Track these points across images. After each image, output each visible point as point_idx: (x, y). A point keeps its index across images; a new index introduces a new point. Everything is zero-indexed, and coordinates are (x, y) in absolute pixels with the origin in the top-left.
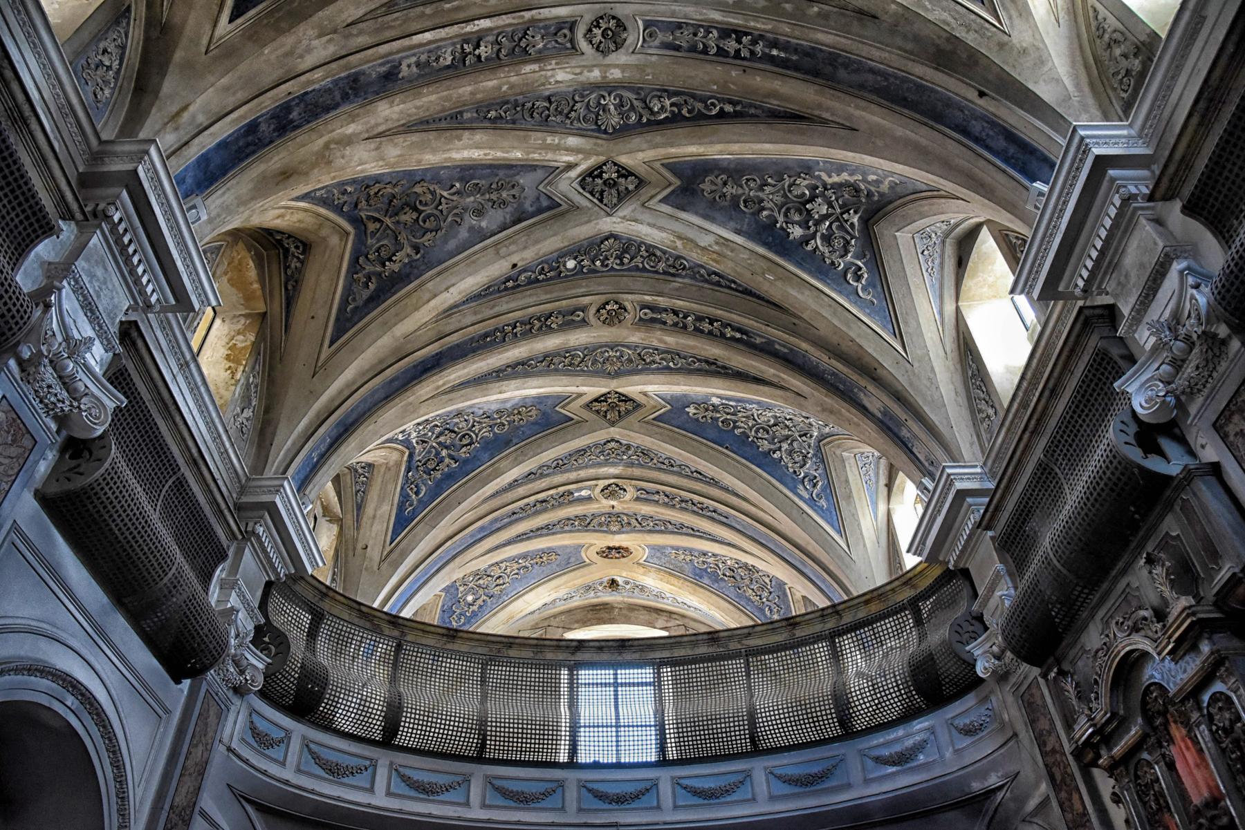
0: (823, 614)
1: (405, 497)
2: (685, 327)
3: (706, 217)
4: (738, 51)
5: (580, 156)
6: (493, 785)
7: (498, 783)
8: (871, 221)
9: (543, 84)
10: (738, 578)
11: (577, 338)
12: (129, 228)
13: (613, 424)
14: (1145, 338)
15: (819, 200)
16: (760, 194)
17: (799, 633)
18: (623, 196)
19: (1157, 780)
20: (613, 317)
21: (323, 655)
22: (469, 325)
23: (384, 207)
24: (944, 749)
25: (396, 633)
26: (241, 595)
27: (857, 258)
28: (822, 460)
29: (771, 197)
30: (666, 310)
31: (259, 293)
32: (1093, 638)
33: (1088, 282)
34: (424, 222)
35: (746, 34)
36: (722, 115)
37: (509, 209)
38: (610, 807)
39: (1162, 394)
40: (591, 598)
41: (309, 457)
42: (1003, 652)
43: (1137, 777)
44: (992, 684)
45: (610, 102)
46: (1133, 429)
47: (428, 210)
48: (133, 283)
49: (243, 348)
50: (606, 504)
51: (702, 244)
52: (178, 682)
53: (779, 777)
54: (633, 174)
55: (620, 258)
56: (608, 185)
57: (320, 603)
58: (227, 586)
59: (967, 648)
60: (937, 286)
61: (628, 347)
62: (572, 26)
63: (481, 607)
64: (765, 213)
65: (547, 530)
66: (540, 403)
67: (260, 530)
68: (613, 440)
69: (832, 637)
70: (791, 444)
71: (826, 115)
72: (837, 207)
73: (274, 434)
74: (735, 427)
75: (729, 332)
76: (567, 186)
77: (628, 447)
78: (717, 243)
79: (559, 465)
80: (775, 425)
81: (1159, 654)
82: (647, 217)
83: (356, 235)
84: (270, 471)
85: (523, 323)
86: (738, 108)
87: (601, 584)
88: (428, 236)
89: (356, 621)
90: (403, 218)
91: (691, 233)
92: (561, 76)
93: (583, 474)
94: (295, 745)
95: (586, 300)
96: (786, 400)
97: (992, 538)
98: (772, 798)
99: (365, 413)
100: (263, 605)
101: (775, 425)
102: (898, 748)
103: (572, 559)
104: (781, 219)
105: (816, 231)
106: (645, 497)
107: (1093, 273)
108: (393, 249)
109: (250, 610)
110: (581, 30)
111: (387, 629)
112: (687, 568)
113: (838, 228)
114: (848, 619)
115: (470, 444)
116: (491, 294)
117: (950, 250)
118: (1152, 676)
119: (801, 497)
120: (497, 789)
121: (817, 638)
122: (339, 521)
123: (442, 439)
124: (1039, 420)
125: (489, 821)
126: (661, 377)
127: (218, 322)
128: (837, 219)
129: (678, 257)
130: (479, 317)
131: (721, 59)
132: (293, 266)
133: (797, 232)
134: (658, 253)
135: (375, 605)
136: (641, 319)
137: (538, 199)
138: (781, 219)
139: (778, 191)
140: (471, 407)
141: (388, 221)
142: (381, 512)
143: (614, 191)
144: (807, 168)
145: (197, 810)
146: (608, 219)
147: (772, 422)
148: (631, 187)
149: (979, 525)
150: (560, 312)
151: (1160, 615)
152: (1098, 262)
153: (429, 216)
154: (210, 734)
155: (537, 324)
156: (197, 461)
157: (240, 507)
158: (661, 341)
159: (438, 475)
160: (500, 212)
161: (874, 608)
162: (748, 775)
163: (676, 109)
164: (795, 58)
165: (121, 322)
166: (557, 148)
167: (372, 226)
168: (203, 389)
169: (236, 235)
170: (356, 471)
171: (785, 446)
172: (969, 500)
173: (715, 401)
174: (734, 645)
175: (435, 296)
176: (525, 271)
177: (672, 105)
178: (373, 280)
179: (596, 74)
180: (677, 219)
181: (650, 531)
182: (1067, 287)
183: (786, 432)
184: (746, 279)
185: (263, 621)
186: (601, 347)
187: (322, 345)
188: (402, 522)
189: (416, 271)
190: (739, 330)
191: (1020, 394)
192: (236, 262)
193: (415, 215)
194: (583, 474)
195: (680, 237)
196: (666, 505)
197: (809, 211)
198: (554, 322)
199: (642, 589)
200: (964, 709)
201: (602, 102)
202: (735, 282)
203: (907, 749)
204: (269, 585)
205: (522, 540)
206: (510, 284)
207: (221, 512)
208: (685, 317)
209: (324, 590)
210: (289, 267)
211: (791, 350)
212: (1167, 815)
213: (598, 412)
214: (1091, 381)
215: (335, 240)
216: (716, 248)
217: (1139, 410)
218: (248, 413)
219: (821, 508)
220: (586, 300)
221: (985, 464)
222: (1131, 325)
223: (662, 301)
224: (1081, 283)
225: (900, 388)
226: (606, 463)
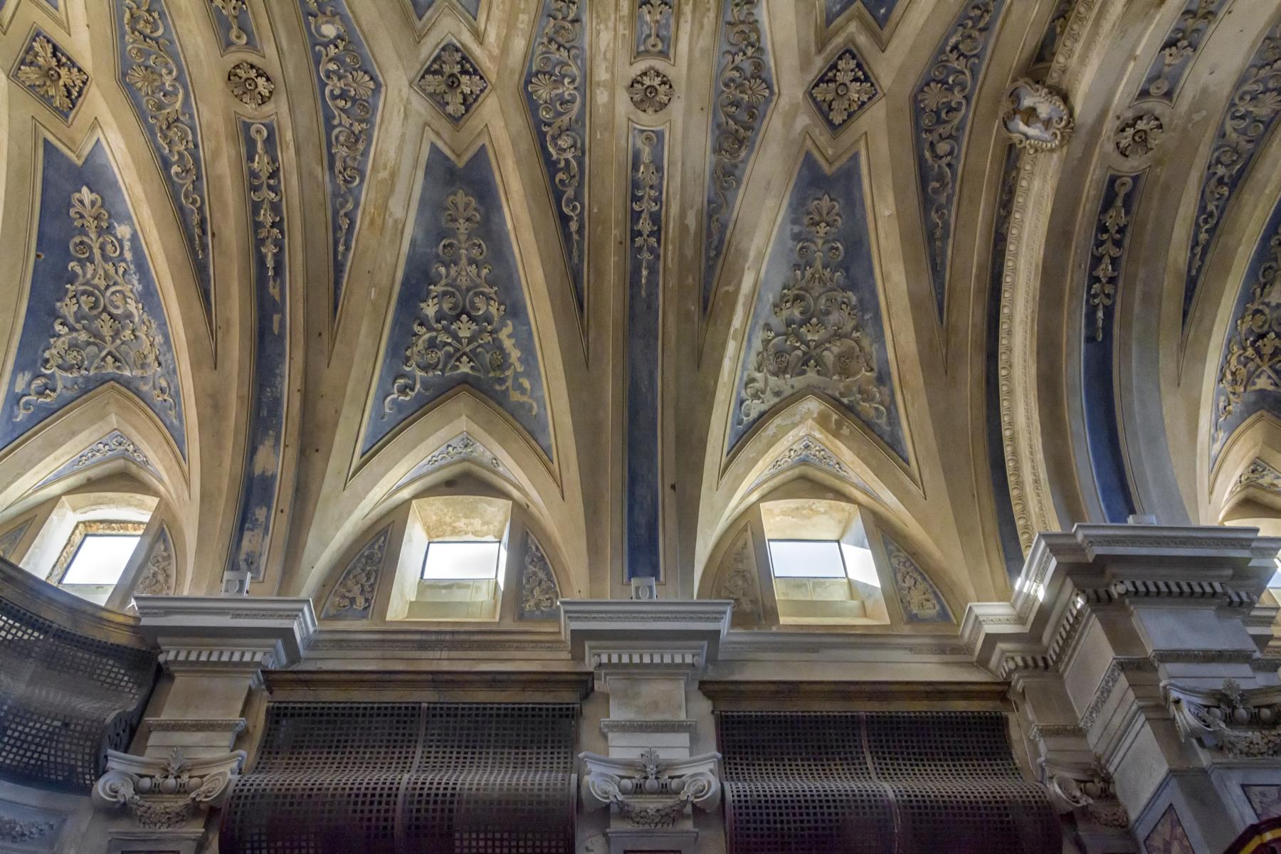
2: (255, 189)
3: (423, 202)
4: (640, 234)
5: (496, 52)
8: (467, 387)
9: (598, 16)
15: (474, 327)
16: (464, 261)
18: (438, 101)
20: (242, 82)
27: (422, 383)
28: (87, 388)
29: (466, 274)
30: (274, 160)
35: (659, 242)
36: (564, 220)
45: (567, 90)
54: (467, 111)
55: (343, 95)
56: (451, 77)
62: (664, 54)
64: (443, 270)
70: (89, 344)
71: (592, 333)
72: (471, 347)
74: (82, 263)
76: (448, 27)
78: (396, 221)
80: (112, 316)
82: (412, 129)
86: (575, 237)
91: (401, 187)
92: (605, 38)
95: (270, 50)
101: (112, 316)
105: (434, 330)
110: (659, 64)
117: (456, 469)
119: (12, 382)
126: (146, 154)
128: (457, 350)
131: (629, 217)
133: (430, 309)
134: (361, 146)
139: (472, 280)
143: (443, 87)
144: (515, 311)
148: (450, 109)
163: (562, 164)
164: (643, 293)
166: (510, 23)
173: (123, 231)
177: (567, 161)
179: (602, 74)
180: (415, 167)
183: (107, 332)
191: (434, 637)
195: (393, 175)
201: (566, 81)
202: (348, 248)
208: (270, 188)
211: (281, 337)
219: (11, 416)
220: (270, 50)
223: (287, 157)
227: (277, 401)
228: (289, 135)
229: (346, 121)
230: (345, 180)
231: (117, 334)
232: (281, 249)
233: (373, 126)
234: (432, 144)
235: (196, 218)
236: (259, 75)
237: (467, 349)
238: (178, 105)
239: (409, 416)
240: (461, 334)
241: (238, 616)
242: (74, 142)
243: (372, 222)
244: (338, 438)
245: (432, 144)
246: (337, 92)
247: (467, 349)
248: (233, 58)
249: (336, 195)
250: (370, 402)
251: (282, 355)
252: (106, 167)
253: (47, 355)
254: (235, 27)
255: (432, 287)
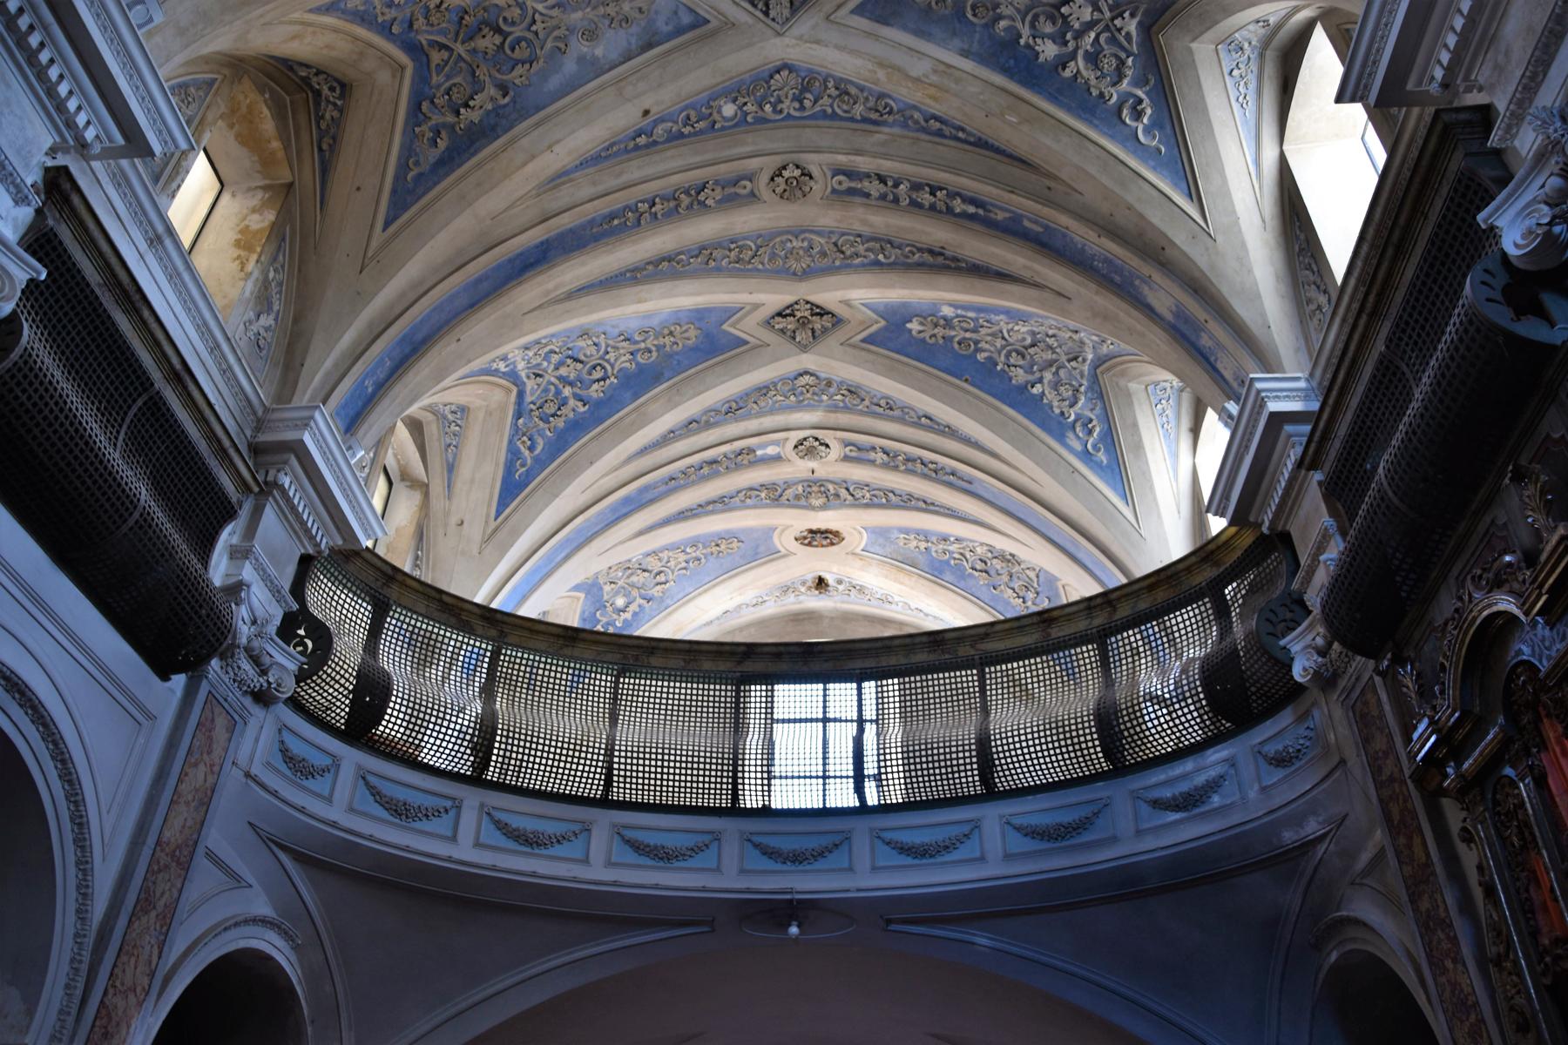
0: (1089, 604)
1: (514, 454)
2: (896, 200)
3: (919, 33)
6: (623, 837)
7: (629, 834)
8: (1155, 29)
10: (992, 572)
11: (745, 221)
12: (37, 24)
13: (804, 348)
14: (1527, 141)
17: (1056, 632)
19: (1523, 803)
21: (392, 659)
22: (586, 200)
23: (453, 28)
24: (1246, 786)
25: (493, 633)
26: (260, 569)
27: (1137, 83)
28: (1099, 394)
30: (868, 176)
31: (281, 154)
32: (1445, 606)
33: (1450, 70)
34: (513, 49)
37: (634, 29)
38: (784, 867)
39: (1546, 220)
40: (792, 603)
41: (360, 384)
42: (1330, 645)
43: (1496, 803)
44: (1315, 693)
46: (1501, 279)
47: (518, 31)
48: (55, 109)
49: (258, 231)
50: (800, 468)
51: (914, 74)
52: (164, 676)
53: (1018, 829)
57: (384, 586)
58: (240, 554)
59: (1282, 643)
60: (1252, 123)
61: (819, 233)
63: (635, 614)
64: (1003, 24)
65: (721, 503)
66: (700, 319)
67: (286, 481)
68: (806, 373)
69: (1101, 638)
72: (1105, 9)
73: (306, 351)
74: (978, 350)
75: (958, 205)
77: (829, 384)
78: (935, 71)
79: (733, 409)
80: (1033, 345)
81: (1527, 614)
83: (416, 71)
84: (303, 397)
85: (664, 199)
87: (804, 583)
88: (519, 70)
89: (436, 614)
90: (481, 43)
91: (899, 58)
93: (768, 422)
94: (347, 774)
95: (754, 163)
96: (1043, 306)
97: (1320, 483)
98: (1008, 857)
99: (440, 329)
100: (298, 589)
102: (1184, 787)
103: (762, 549)
104: (1026, 32)
106: (859, 454)
107: (1457, 55)
108: (469, 91)
109: (275, 591)
111: (478, 624)
112: (922, 560)
113: (1108, 41)
114: (1124, 611)
115: (604, 379)
116: (616, 154)
117: (1271, 70)
118: (1520, 652)
120: (628, 842)
121: (1082, 640)
122: (424, 488)
123: (563, 371)
124: (1380, 295)
125: (615, 883)
127: (225, 198)
129: (881, 96)
130: (601, 188)
132: (328, 116)
133: (1049, 50)
134: (853, 91)
135: (478, 599)
136: (834, 191)
137: (676, 13)
138: (1026, 32)
140: (599, 323)
141: (460, 49)
142: (480, 472)
145: (200, 850)
146: (778, 41)
147: (1029, 341)
149: (1300, 464)
150: (717, 182)
151: (1530, 558)
152: (1464, 38)
153: (518, 41)
154: (218, 751)
155: (686, 200)
156: (181, 376)
157: (256, 450)
158: (864, 222)
159: (560, 423)
160: (622, 32)
161: (1161, 595)
162: (976, 825)
165: (47, 170)
167: (437, 57)
168: (186, 277)
169: (237, 66)
170: (445, 417)
171: (1048, 376)
172: (1288, 428)
173: (947, 311)
174: (965, 651)
175: (533, 157)
176: (662, 120)
178: (444, 134)
180: (877, 37)
181: (867, 506)
182: (1420, 83)
183: (1049, 356)
184: (979, 124)
185: (295, 607)
186: (780, 234)
187: (372, 226)
188: (512, 488)
189: (504, 122)
190: (972, 201)
191: (1359, 263)
192: (244, 109)
193: (498, 39)
194: (768, 422)
195: (881, 65)
196: (885, 466)
197: (1062, 15)
198: (709, 196)
199: (861, 590)
200: (1277, 730)
202: (963, 130)
203: (1196, 789)
204: (306, 562)
205: (686, 518)
206: (642, 140)
207: (224, 451)
208: (896, 185)
209: (390, 572)
210: (323, 117)
211: (1046, 227)
212: (1533, 854)
213: (783, 331)
214: (1451, 223)
215: (384, 77)
216: (934, 78)
217: (1512, 251)
218: (267, 320)
221: (1312, 375)
222: (1509, 127)
223: (864, 163)
224: (1439, 74)
225: (1197, 274)
226: (799, 406)
227: (1106, 261)
228: (842, 158)
229: (826, 100)
230: (890, 113)
231: (1050, 347)
232: (958, 194)
233: (829, 75)
234: (852, 12)
235: (927, 257)
236: (780, 175)
237: (1108, 15)
238: (822, 241)
239: (1171, 121)
240: (1088, 18)
241: (1247, 447)
242: (862, 322)
243: (935, 99)
244: (1155, 221)
245: (852, 12)
246: (797, 105)
247: (1108, 15)
248: (765, 193)
249: (905, 126)
250: (1133, 163)
251: (1064, 236)
252: (886, 305)
253: (1057, 411)
254: (732, 190)
255: (1022, 42)
